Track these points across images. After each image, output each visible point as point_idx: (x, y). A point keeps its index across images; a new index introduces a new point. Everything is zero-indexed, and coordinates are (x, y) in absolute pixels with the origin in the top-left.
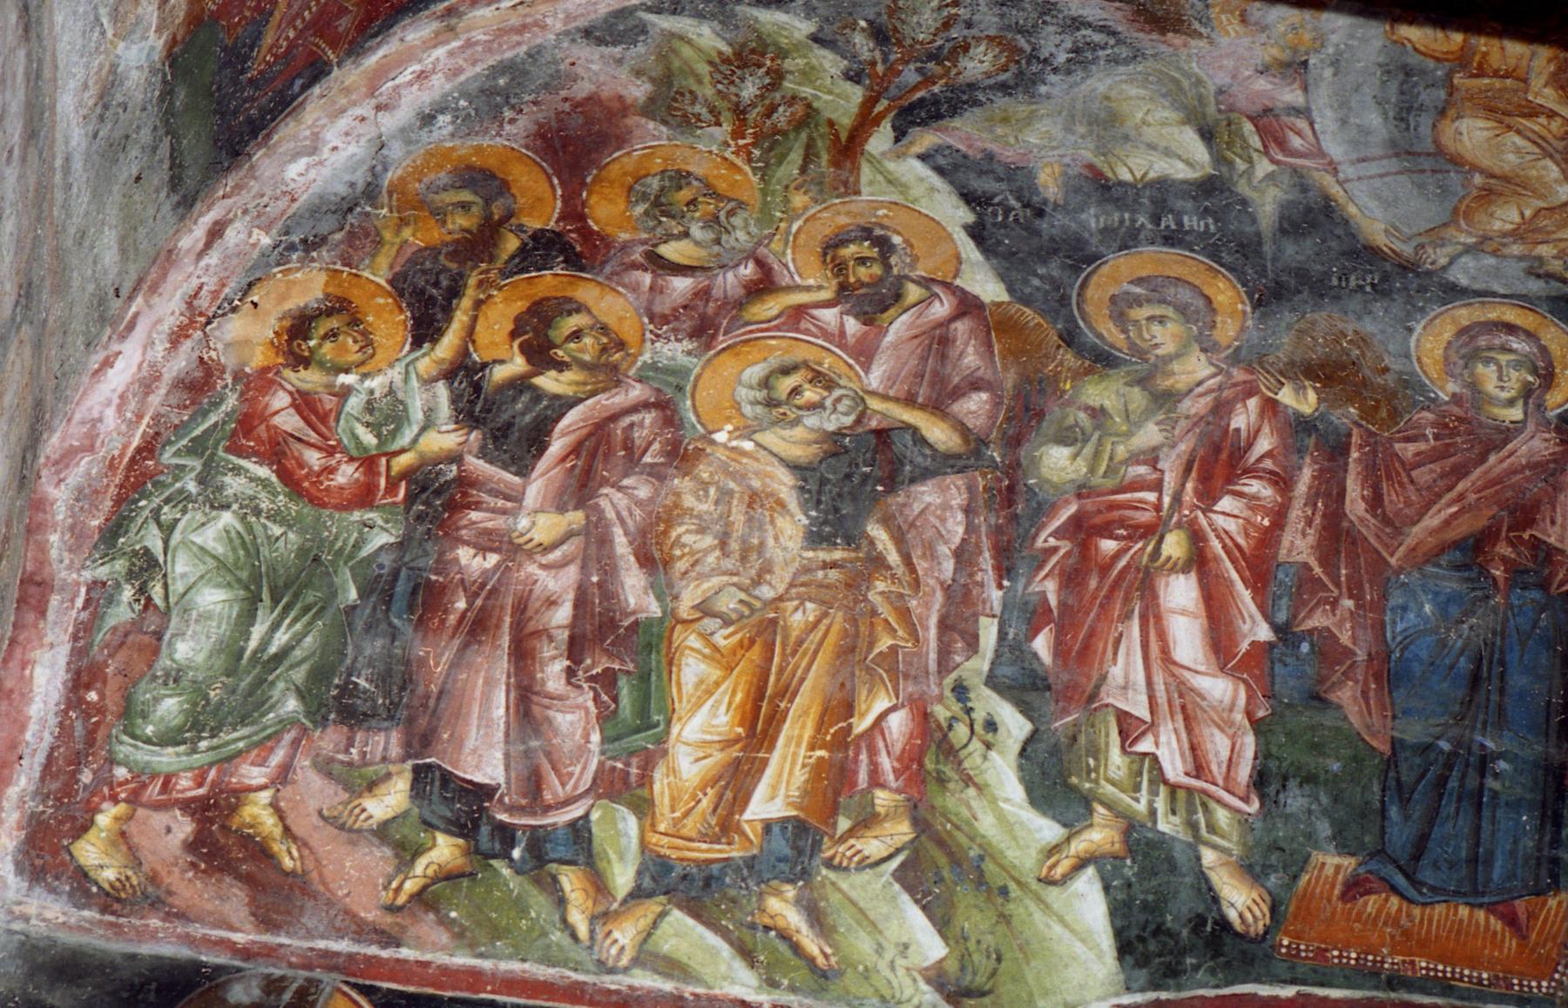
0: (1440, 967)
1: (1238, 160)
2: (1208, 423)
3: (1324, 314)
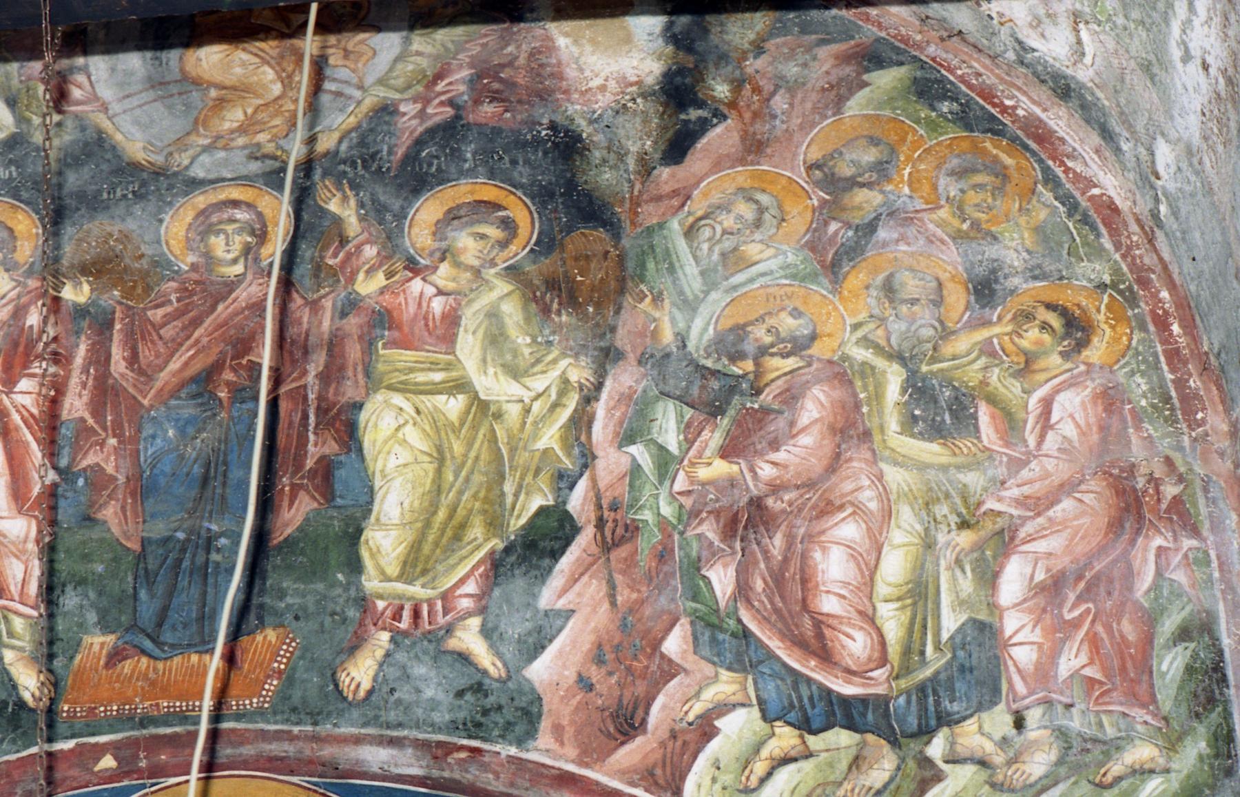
0: (178, 704)
1: (34, 117)
2: (10, 326)
3: (97, 223)
